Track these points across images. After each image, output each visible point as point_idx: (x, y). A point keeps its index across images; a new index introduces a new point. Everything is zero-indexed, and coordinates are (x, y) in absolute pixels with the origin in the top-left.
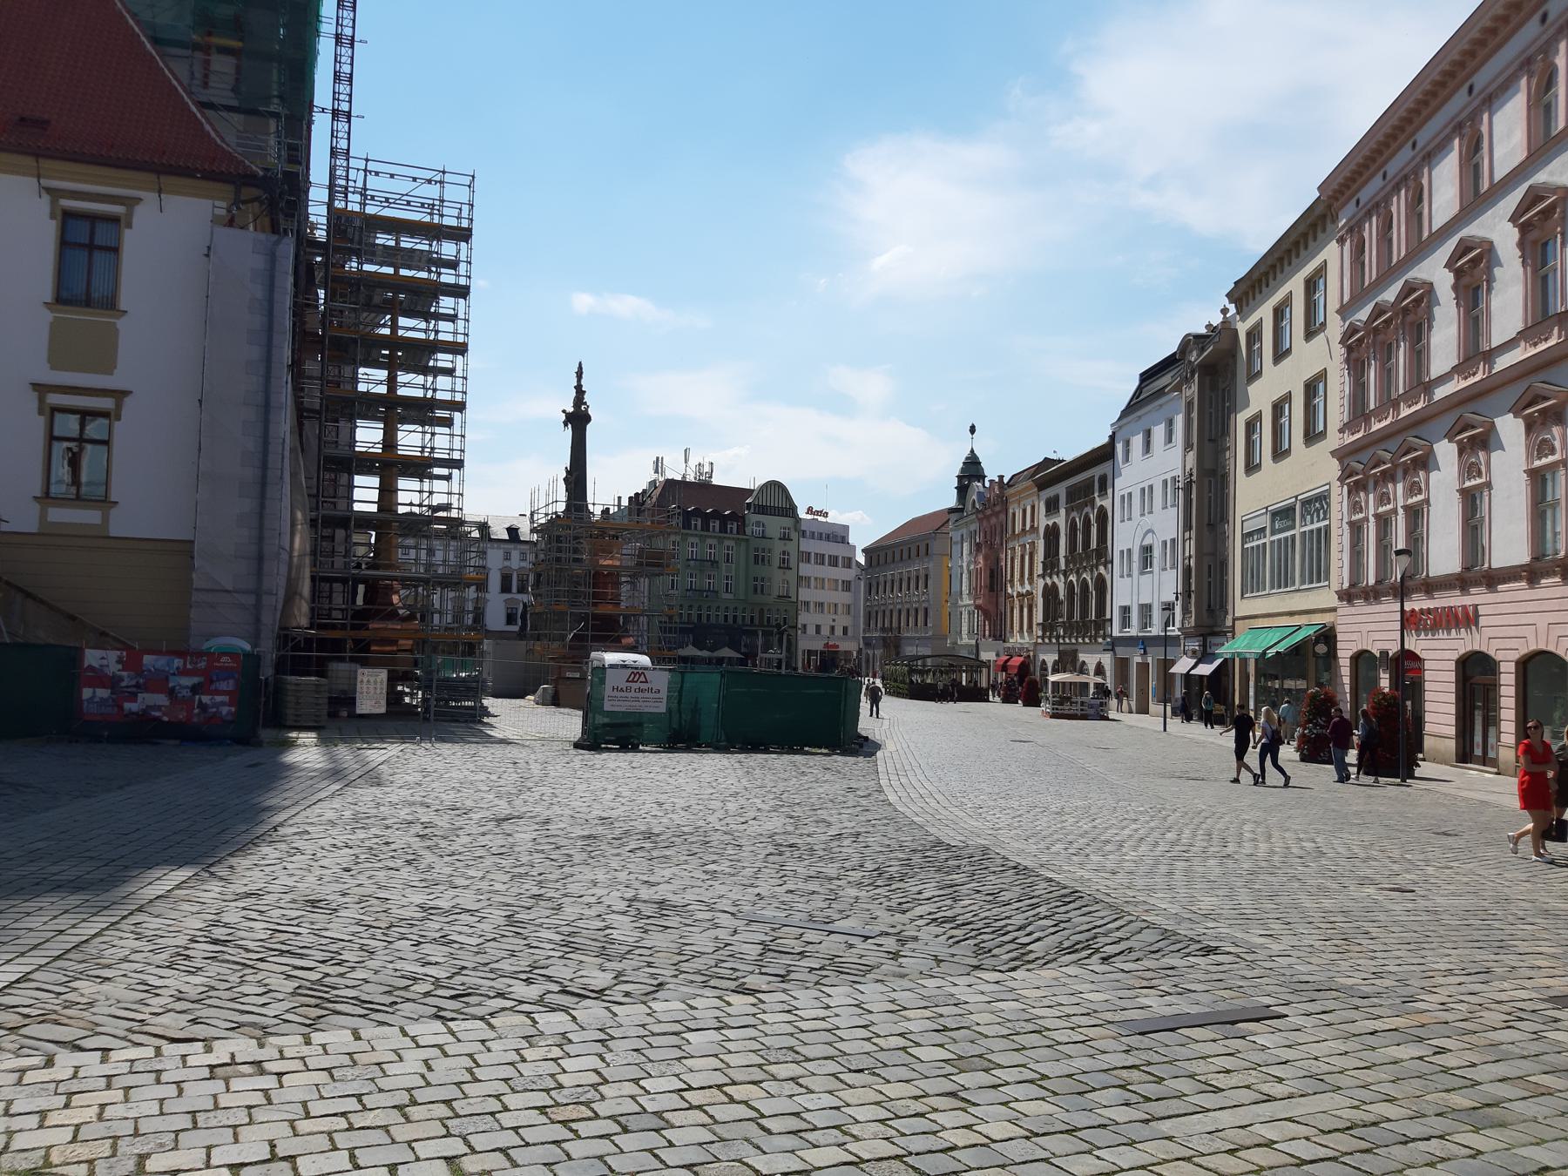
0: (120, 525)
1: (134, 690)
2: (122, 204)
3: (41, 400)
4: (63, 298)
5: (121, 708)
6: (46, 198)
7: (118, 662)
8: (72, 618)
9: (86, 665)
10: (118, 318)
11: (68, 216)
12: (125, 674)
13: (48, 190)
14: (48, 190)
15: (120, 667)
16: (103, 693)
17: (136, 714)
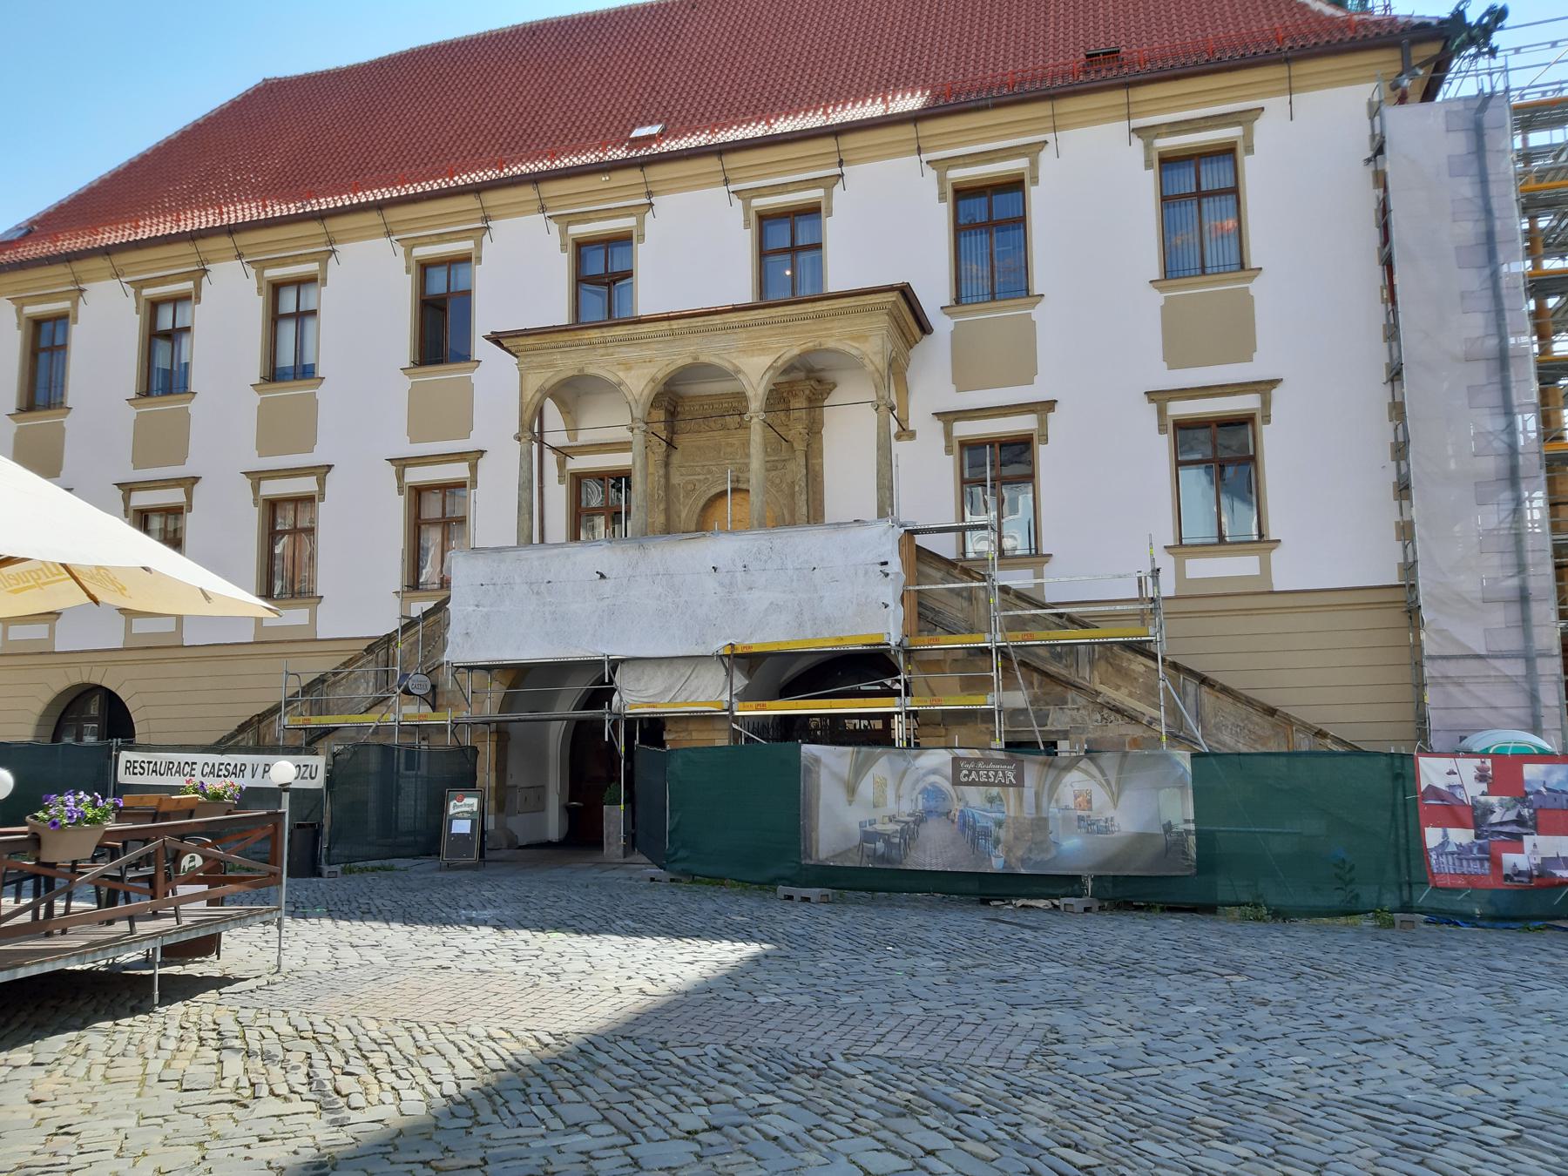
0: (1288, 573)
1: (1514, 829)
2: (1239, 123)
3: (1161, 412)
4: (1171, 271)
5: (1496, 863)
6: (1138, 143)
7: (1481, 778)
8: (1271, 712)
9: (1423, 788)
10: (1250, 279)
11: (1168, 162)
12: (1494, 800)
13: (1137, 131)
14: (1137, 131)
15: (1484, 787)
16: (1461, 836)
17: (1529, 874)
